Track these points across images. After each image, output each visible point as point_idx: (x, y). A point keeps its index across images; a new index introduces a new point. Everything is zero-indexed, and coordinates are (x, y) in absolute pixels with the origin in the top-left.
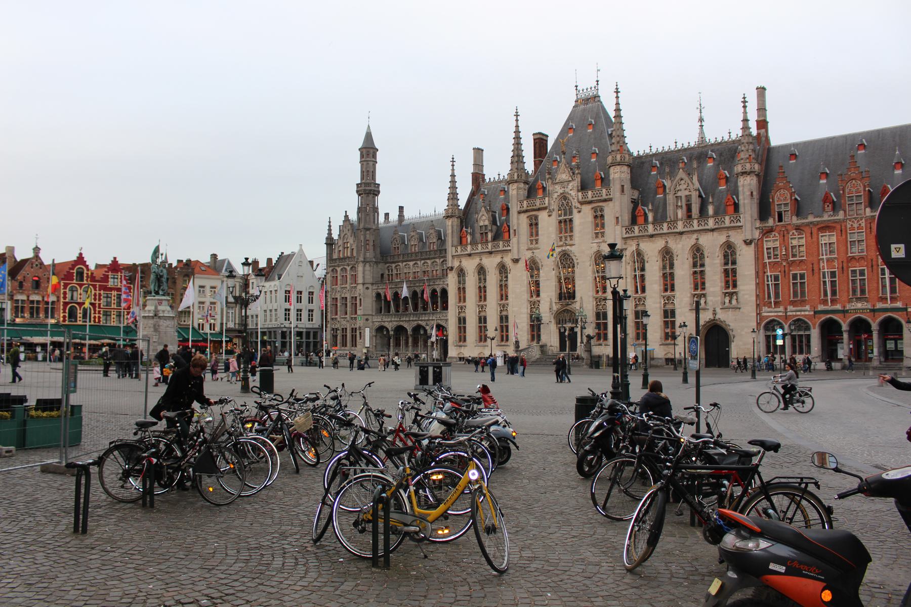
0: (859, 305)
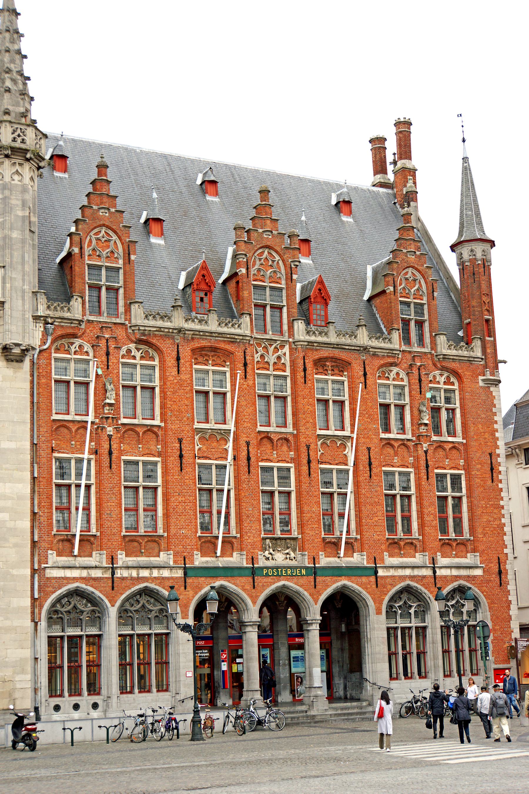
0: (280, 558)
